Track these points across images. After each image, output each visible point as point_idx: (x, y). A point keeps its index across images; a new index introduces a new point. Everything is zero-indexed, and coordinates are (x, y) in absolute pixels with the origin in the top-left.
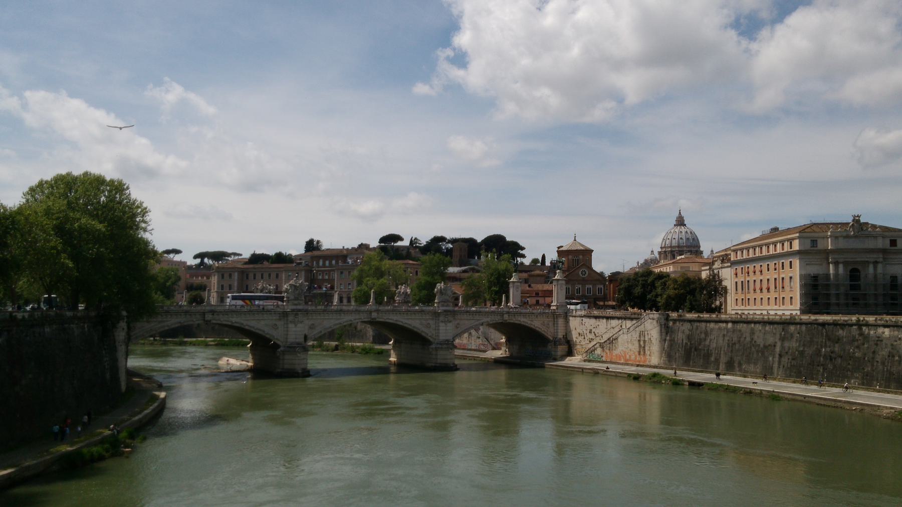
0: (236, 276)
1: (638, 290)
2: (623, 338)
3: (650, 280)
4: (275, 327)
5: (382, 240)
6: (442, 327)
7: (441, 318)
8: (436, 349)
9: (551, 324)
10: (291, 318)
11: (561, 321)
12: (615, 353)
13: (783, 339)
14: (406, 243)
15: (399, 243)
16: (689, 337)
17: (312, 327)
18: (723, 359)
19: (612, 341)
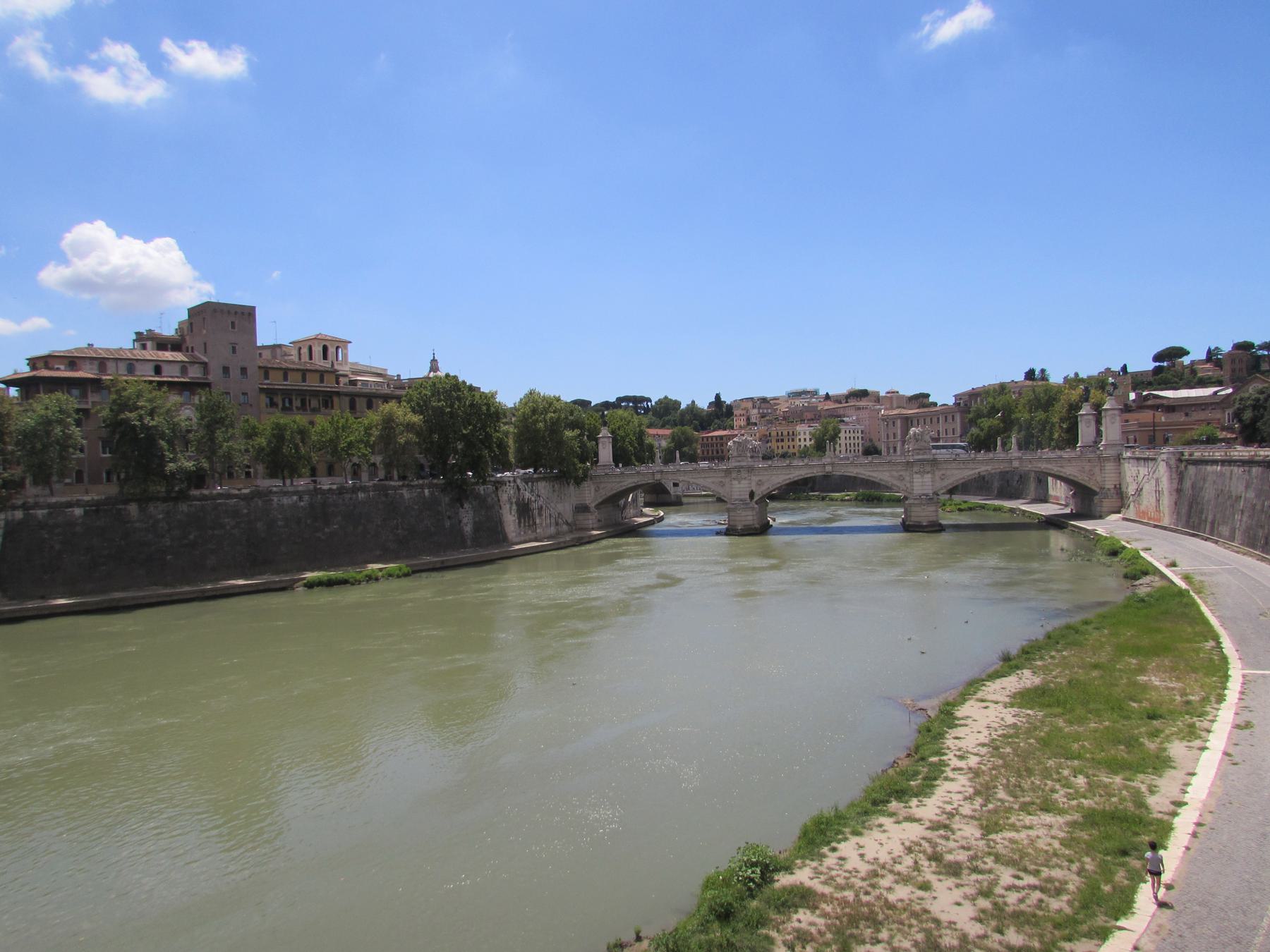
0: (899, 423)
1: (1248, 415)
2: (1148, 488)
3: (1262, 397)
4: (722, 484)
5: (1158, 357)
6: (917, 479)
7: (915, 469)
8: (910, 505)
9: (1097, 470)
10: (734, 475)
11: (1110, 466)
12: (1142, 508)
13: (1247, 487)
14: (1197, 353)
15: (1186, 360)
16: (1193, 487)
17: (760, 483)
18: (1210, 518)
19: (1139, 491)
